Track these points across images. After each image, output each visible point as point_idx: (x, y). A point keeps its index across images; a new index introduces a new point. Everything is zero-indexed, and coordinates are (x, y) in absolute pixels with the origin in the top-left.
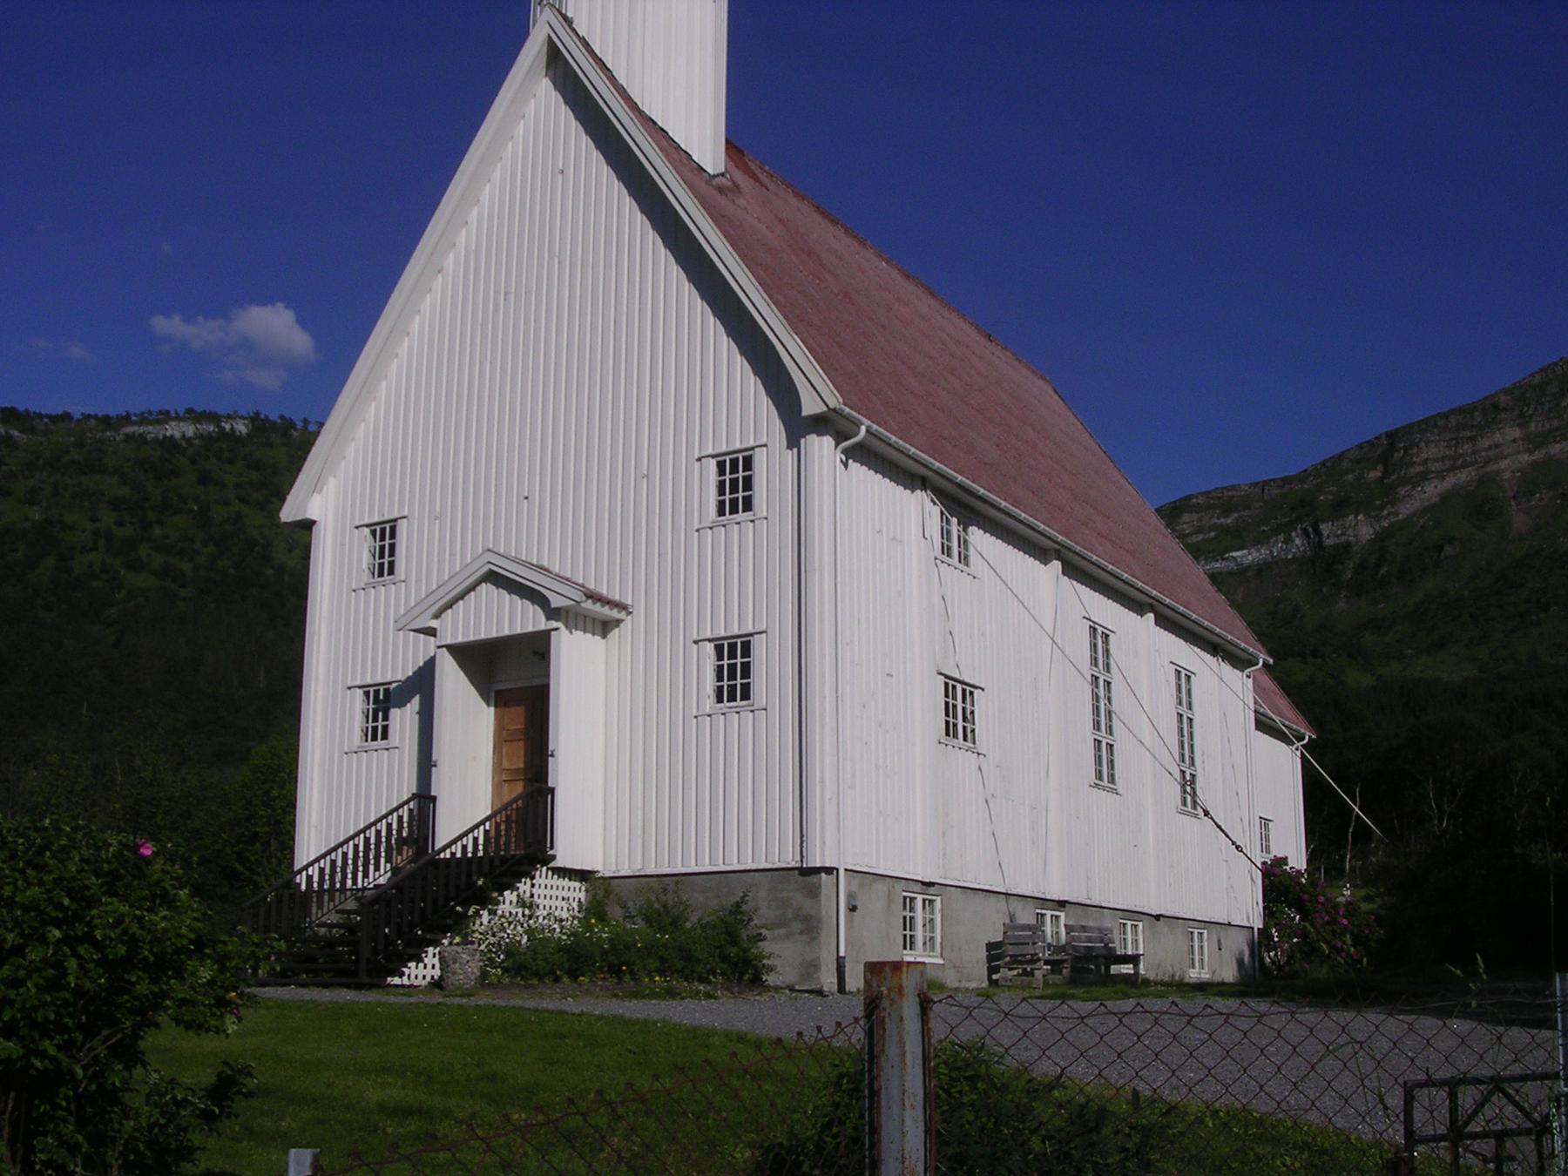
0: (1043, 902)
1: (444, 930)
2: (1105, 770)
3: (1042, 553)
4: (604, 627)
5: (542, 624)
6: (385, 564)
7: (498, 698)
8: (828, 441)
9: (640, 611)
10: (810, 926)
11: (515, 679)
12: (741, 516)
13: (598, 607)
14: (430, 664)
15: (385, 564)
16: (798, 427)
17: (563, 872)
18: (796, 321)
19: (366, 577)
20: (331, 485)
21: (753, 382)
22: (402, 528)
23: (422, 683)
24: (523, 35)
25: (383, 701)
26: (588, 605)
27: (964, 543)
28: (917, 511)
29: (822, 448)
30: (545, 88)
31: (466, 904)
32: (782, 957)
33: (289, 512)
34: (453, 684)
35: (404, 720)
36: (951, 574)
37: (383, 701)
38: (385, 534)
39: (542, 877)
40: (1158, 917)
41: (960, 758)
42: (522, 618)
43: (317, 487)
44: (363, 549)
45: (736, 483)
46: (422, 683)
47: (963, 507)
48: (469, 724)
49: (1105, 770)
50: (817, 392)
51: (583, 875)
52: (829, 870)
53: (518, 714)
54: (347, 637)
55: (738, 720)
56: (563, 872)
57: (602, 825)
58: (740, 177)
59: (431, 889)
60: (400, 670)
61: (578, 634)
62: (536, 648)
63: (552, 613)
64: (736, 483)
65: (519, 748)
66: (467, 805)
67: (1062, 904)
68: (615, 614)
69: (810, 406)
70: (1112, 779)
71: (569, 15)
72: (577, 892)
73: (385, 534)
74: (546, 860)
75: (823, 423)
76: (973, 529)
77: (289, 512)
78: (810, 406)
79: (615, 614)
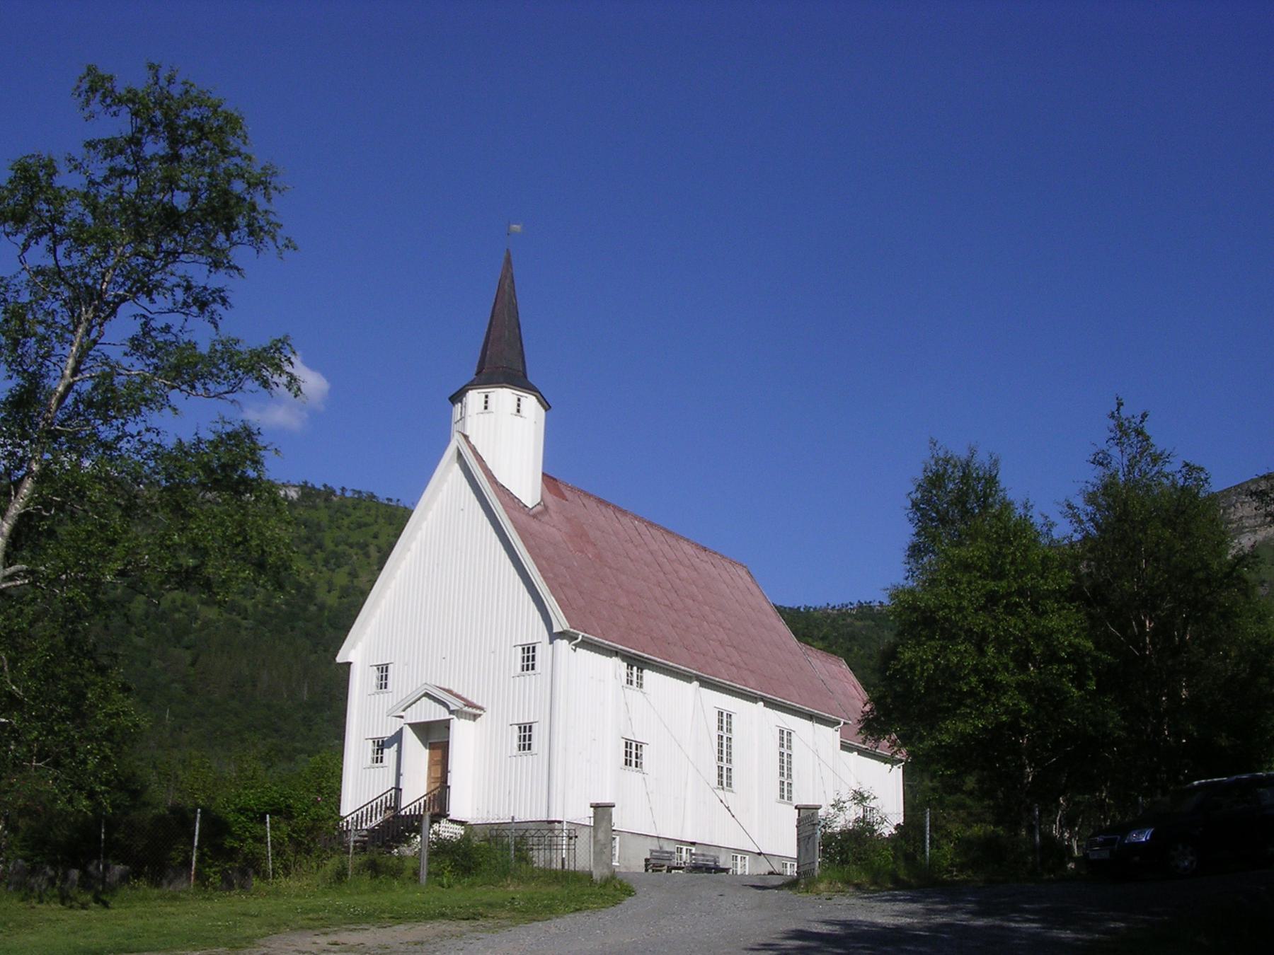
0: (682, 842)
1: (399, 842)
2: (724, 778)
3: (688, 678)
4: (475, 717)
5: (447, 716)
6: (383, 684)
7: (432, 747)
8: (565, 642)
9: (489, 711)
10: (550, 846)
11: (435, 737)
12: (530, 672)
13: (470, 710)
14: (399, 735)
15: (383, 684)
16: (553, 637)
17: (453, 821)
18: (553, 591)
19: (374, 689)
20: (360, 646)
21: (537, 613)
22: (391, 667)
23: (398, 738)
24: (449, 441)
25: (381, 745)
26: (466, 709)
27: (640, 678)
28: (617, 666)
29: (563, 644)
30: (456, 467)
31: (410, 832)
32: (539, 858)
33: (340, 658)
34: (410, 738)
35: (390, 754)
36: (633, 692)
37: (381, 745)
38: (383, 669)
39: (444, 822)
40: (760, 854)
41: (632, 774)
42: (439, 713)
43: (353, 647)
44: (374, 675)
45: (529, 657)
46: (398, 738)
47: (636, 662)
48: (417, 755)
49: (724, 778)
50: (560, 622)
51: (462, 823)
52: (559, 822)
53: (439, 752)
54: (366, 715)
55: (526, 758)
56: (453, 821)
57: (471, 803)
58: (550, 499)
59: (397, 826)
60: (389, 733)
61: (462, 720)
62: (446, 725)
63: (451, 712)
64: (529, 657)
65: (439, 768)
66: (415, 790)
67: (693, 844)
68: (478, 712)
69: (556, 629)
70: (729, 785)
71: (467, 433)
72: (460, 830)
73: (383, 669)
74: (446, 816)
75: (562, 635)
76: (646, 672)
77: (340, 658)
78: (556, 629)
79: (478, 712)
